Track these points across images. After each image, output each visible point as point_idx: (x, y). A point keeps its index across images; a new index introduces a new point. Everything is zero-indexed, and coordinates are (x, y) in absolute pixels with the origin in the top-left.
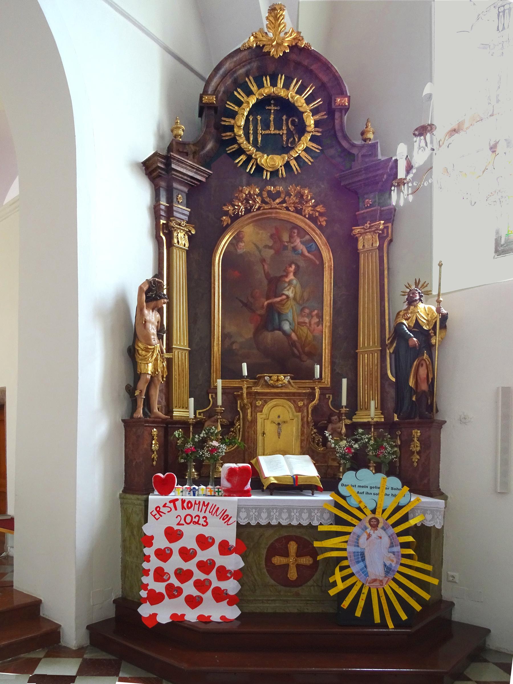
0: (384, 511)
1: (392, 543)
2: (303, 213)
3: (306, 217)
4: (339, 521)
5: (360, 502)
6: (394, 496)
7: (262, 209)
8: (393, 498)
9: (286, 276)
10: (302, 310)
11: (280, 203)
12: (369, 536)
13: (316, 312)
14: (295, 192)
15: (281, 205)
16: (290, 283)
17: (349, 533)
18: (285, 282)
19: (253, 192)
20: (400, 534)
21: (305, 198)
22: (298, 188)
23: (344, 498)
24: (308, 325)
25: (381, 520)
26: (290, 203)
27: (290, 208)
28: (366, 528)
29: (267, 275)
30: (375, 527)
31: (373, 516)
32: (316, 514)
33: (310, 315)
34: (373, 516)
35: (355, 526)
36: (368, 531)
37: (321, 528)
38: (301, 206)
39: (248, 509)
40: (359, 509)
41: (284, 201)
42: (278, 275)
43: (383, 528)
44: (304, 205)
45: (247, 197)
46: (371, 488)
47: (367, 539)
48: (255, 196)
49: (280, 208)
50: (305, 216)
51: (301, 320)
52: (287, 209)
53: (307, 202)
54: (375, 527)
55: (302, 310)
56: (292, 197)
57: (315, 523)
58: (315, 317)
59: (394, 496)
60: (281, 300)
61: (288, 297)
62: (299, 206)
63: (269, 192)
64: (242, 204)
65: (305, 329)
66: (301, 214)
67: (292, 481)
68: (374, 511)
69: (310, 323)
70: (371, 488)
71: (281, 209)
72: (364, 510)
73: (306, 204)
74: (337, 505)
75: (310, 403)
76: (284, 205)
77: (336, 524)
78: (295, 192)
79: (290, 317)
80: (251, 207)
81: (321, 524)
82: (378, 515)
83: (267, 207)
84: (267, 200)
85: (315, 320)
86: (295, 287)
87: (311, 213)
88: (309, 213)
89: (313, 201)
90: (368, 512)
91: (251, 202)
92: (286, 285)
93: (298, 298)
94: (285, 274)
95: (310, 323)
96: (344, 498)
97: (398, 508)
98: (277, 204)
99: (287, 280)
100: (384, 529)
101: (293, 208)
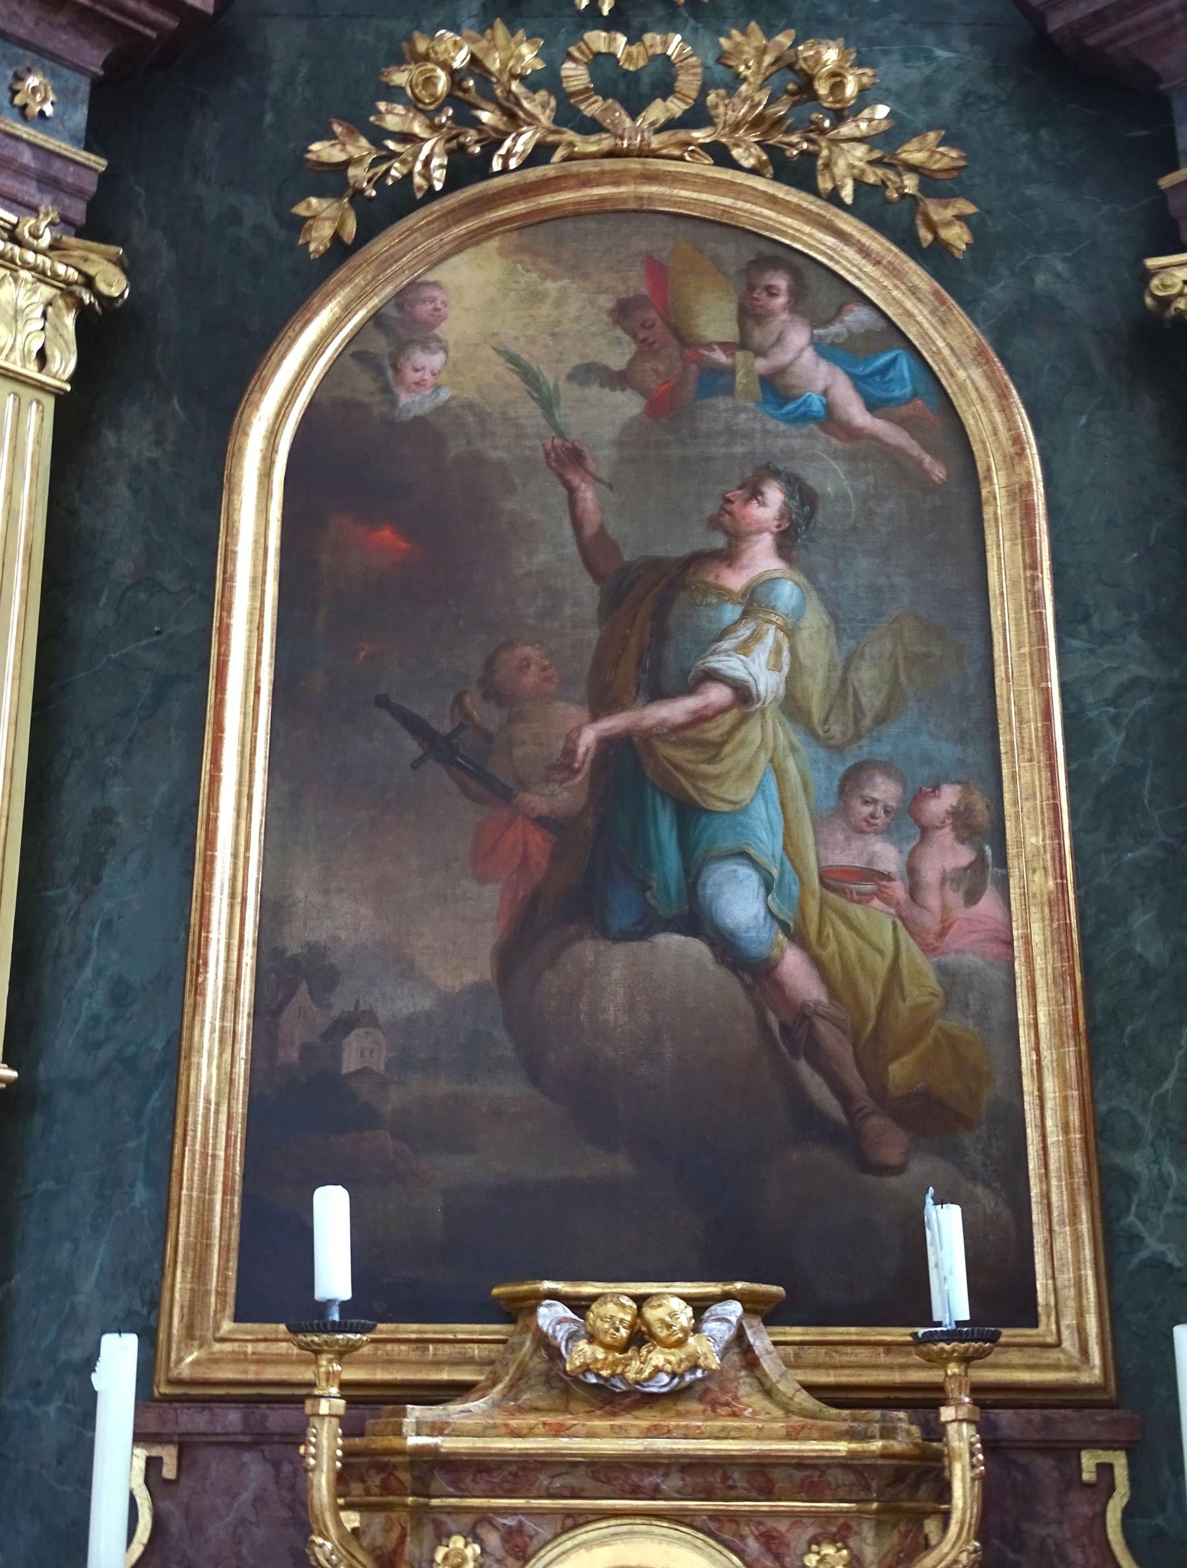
2: (825, 184)
3: (840, 204)
7: (560, 154)
9: (730, 556)
11: (671, 125)
13: (948, 797)
14: (759, 63)
15: (682, 135)
18: (724, 594)
19: (504, 64)
21: (822, 89)
22: (784, 39)
24: (899, 890)
26: (736, 126)
27: (736, 153)
38: (811, 141)
41: (698, 116)
42: (673, 548)
44: (823, 132)
45: (467, 90)
48: (515, 86)
49: (677, 152)
50: (834, 198)
51: (846, 856)
52: (720, 155)
53: (839, 117)
56: (744, 88)
58: (946, 836)
60: (700, 719)
61: (743, 694)
62: (794, 139)
63: (600, 62)
64: (435, 128)
66: (814, 191)
69: (912, 871)
71: (682, 159)
73: (834, 126)
76: (701, 135)
78: (759, 63)
80: (492, 144)
83: (593, 148)
84: (593, 108)
86: (791, 632)
87: (871, 179)
88: (859, 183)
89: (882, 111)
91: (485, 116)
92: (731, 613)
94: (719, 541)
95: (912, 871)
98: (658, 131)
99: (736, 580)
101: (756, 150)
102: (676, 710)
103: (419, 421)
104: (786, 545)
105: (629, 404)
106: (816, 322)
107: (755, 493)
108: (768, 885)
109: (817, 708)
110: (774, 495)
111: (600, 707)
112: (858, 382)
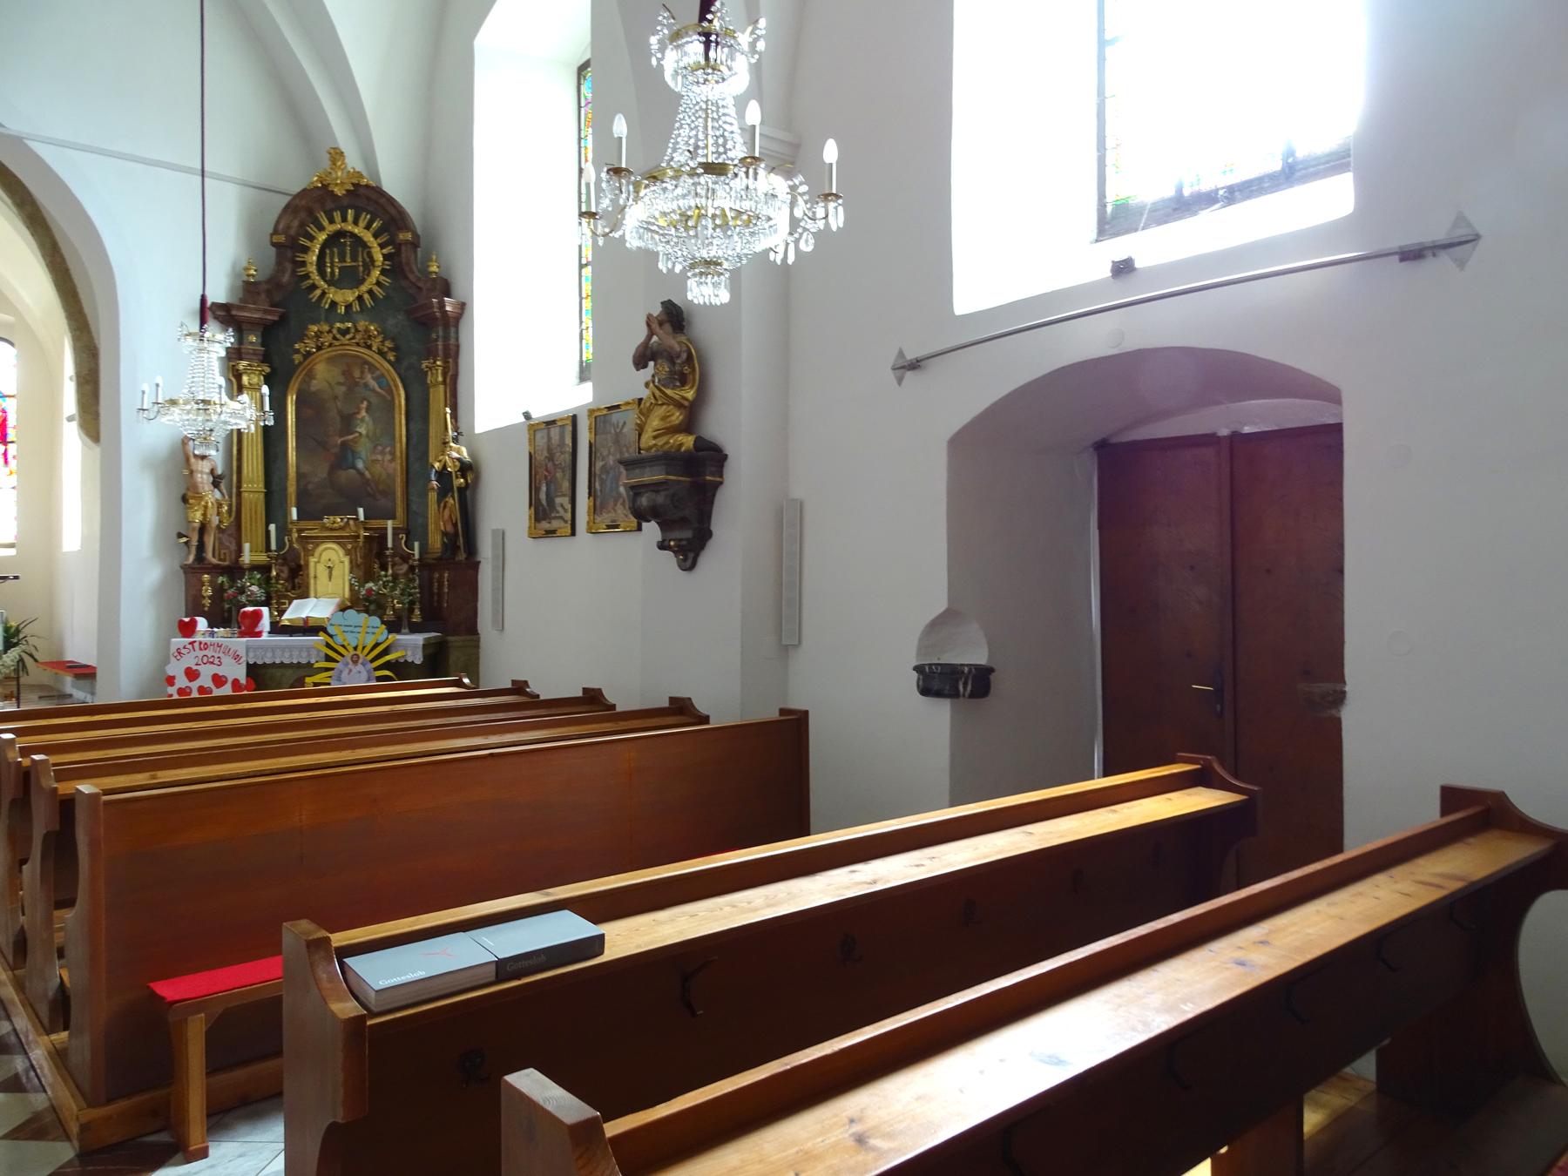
0: (364, 648)
1: (369, 678)
4: (328, 659)
5: (344, 640)
6: (373, 633)
8: (373, 636)
9: (358, 413)
10: (375, 447)
12: (350, 671)
13: (388, 449)
16: (362, 420)
17: (332, 669)
20: (376, 669)
23: (331, 636)
25: (361, 656)
28: (347, 664)
29: (340, 413)
30: (355, 662)
31: (355, 652)
32: (314, 653)
33: (383, 453)
34: (355, 652)
35: (338, 662)
36: (350, 666)
37: (316, 665)
39: (256, 649)
40: (343, 646)
42: (351, 412)
43: (362, 664)
46: (355, 627)
47: (349, 674)
51: (374, 458)
54: (355, 662)
55: (375, 447)
57: (313, 661)
59: (373, 633)
60: (355, 438)
61: (360, 434)
65: (378, 466)
67: (302, 622)
68: (355, 648)
70: (355, 627)
72: (348, 647)
74: (328, 645)
75: (290, 547)
77: (326, 661)
79: (363, 454)
81: (317, 662)
82: (359, 652)
85: (388, 457)
90: (351, 650)
92: (359, 422)
93: (370, 435)
94: (356, 411)
96: (331, 636)
97: (377, 645)
99: (359, 416)
100: (363, 664)
102: (351, 437)
103: (314, 393)
104: (368, 410)
105: (343, 389)
106: (373, 373)
107: (362, 402)
108: (364, 462)
109: (370, 435)
110: (365, 403)
111: (341, 436)
112: (378, 383)
